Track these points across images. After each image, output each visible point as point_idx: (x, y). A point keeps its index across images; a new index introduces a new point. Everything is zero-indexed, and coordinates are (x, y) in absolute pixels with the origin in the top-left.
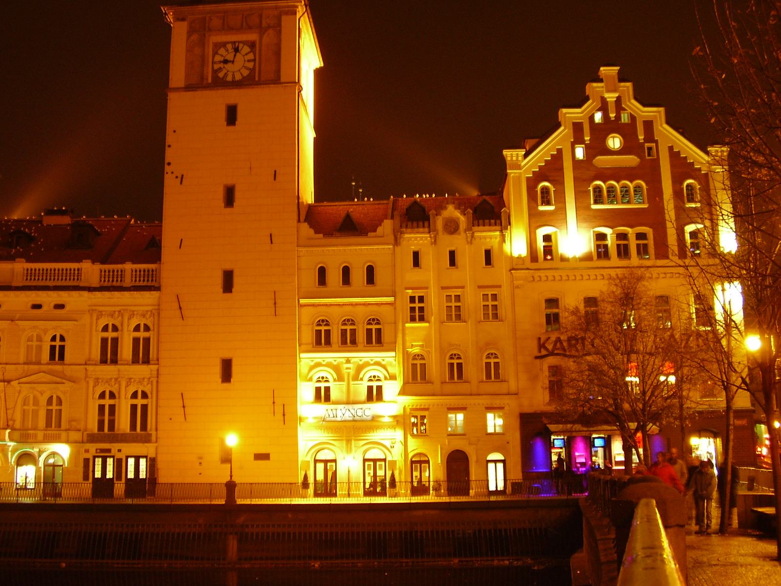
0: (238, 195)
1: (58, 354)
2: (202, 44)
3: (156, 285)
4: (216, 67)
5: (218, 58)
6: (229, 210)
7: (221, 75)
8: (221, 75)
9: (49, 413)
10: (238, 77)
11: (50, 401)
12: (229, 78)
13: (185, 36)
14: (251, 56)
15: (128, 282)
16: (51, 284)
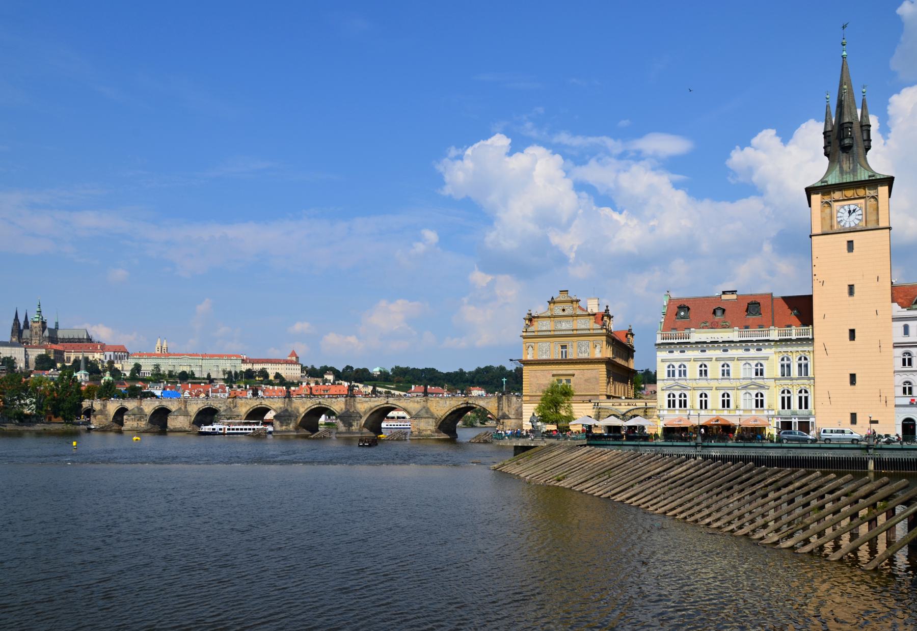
0: (856, 290)
1: (760, 373)
2: (830, 206)
3: (810, 337)
4: (839, 219)
5: (839, 214)
6: (851, 298)
7: (842, 224)
8: (842, 224)
9: (757, 401)
10: (853, 225)
11: (757, 396)
12: (847, 226)
13: (819, 203)
14: (860, 212)
15: (794, 337)
16: (754, 339)
